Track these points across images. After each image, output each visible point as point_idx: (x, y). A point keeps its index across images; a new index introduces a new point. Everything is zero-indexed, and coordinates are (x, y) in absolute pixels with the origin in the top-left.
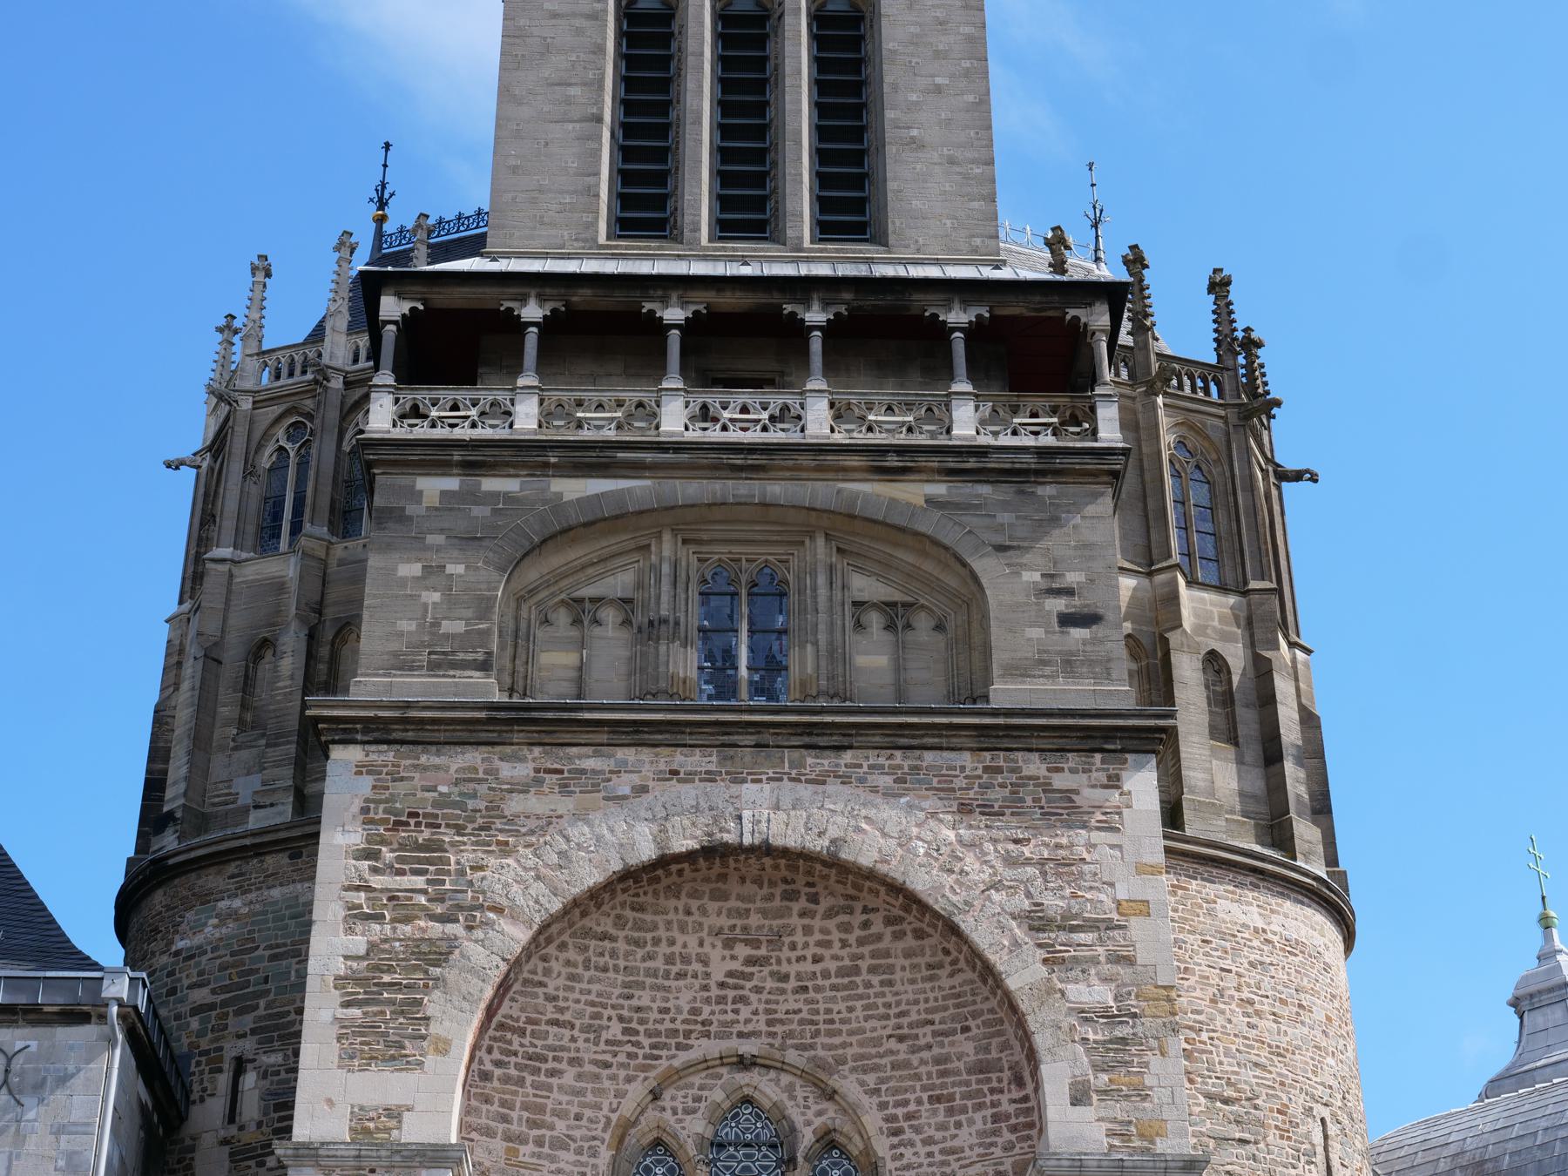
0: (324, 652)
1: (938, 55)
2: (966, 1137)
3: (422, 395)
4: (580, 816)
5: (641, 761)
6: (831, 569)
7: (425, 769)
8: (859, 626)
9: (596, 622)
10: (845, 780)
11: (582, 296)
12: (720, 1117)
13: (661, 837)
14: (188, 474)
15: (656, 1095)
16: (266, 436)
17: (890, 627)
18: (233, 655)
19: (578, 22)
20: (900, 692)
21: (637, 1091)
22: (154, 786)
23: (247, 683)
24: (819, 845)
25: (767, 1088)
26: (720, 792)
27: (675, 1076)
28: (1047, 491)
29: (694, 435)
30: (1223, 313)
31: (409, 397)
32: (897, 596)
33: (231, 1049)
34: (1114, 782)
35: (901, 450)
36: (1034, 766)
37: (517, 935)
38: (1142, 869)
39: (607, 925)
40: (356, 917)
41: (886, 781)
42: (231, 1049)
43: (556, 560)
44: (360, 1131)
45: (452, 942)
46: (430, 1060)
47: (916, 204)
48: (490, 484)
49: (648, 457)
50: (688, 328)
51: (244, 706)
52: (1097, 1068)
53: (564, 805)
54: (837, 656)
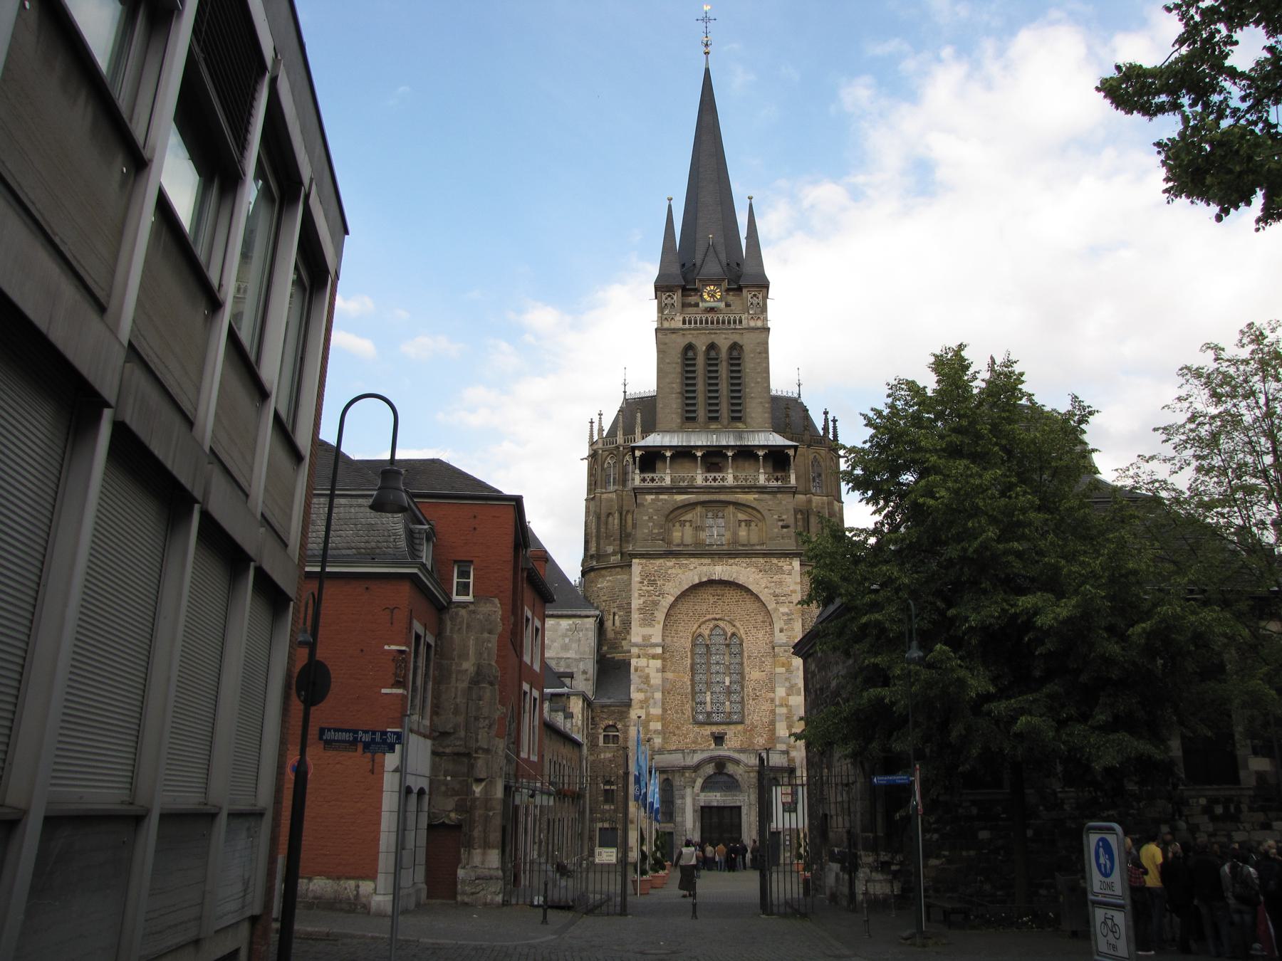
0: (623, 517)
1: (758, 373)
2: (760, 636)
3: (646, 475)
4: (683, 573)
5: (695, 561)
6: (734, 513)
7: (652, 564)
8: (740, 526)
9: (684, 526)
10: (736, 565)
11: (678, 449)
12: (712, 630)
13: (700, 578)
14: (586, 462)
15: (700, 626)
16: (606, 459)
17: (746, 525)
18: (603, 518)
19: (674, 365)
20: (749, 541)
21: (696, 626)
22: (587, 542)
23: (607, 523)
24: (732, 580)
25: (721, 624)
26: (711, 568)
27: (704, 623)
28: (779, 496)
29: (704, 484)
30: (826, 420)
31: (642, 475)
32: (748, 519)
33: (612, 610)
34: (791, 564)
35: (748, 488)
36: (775, 561)
37: (673, 599)
38: (796, 583)
39: (689, 593)
40: (640, 596)
41: (745, 565)
42: (612, 610)
43: (676, 513)
44: (643, 640)
45: (660, 601)
46: (656, 625)
47: (753, 415)
48: (661, 497)
49: (695, 490)
50: (703, 456)
51: (606, 528)
52: (785, 624)
53: (680, 571)
54: (735, 534)
